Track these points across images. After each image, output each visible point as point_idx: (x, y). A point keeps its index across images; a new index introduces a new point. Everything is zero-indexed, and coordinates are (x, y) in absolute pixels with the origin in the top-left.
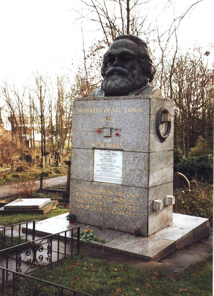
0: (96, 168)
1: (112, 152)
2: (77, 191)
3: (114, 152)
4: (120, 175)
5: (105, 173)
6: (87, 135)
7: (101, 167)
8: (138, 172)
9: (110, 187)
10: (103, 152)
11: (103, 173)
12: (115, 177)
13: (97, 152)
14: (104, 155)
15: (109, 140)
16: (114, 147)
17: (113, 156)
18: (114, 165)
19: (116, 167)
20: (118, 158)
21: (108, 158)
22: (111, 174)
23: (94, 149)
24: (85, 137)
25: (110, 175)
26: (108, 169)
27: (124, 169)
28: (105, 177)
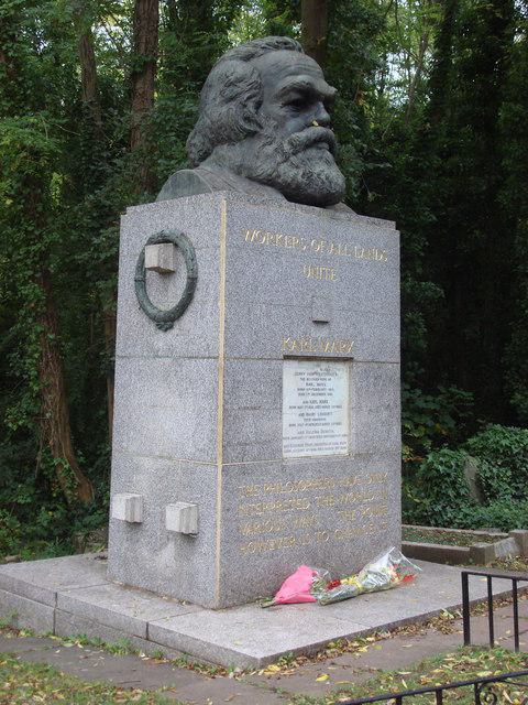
0: (289, 416)
1: (324, 365)
2: (242, 502)
3: (332, 365)
4: (343, 429)
5: (312, 428)
6: (269, 317)
7: (298, 411)
8: (384, 415)
9: (326, 467)
10: (306, 367)
11: (304, 428)
12: (333, 436)
13: (290, 369)
14: (305, 376)
15: (323, 332)
16: (331, 351)
17: (328, 378)
18: (330, 403)
19: (337, 409)
20: (339, 383)
21: (315, 382)
22: (324, 428)
23: (287, 358)
24: (264, 321)
25: (322, 432)
26: (317, 417)
27: (356, 408)
28: (310, 441)
